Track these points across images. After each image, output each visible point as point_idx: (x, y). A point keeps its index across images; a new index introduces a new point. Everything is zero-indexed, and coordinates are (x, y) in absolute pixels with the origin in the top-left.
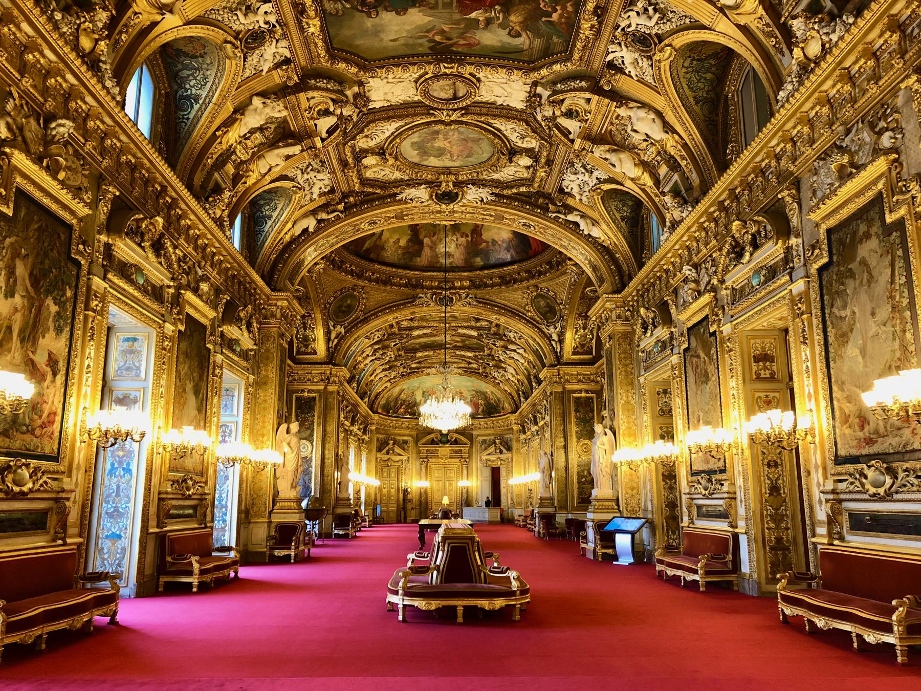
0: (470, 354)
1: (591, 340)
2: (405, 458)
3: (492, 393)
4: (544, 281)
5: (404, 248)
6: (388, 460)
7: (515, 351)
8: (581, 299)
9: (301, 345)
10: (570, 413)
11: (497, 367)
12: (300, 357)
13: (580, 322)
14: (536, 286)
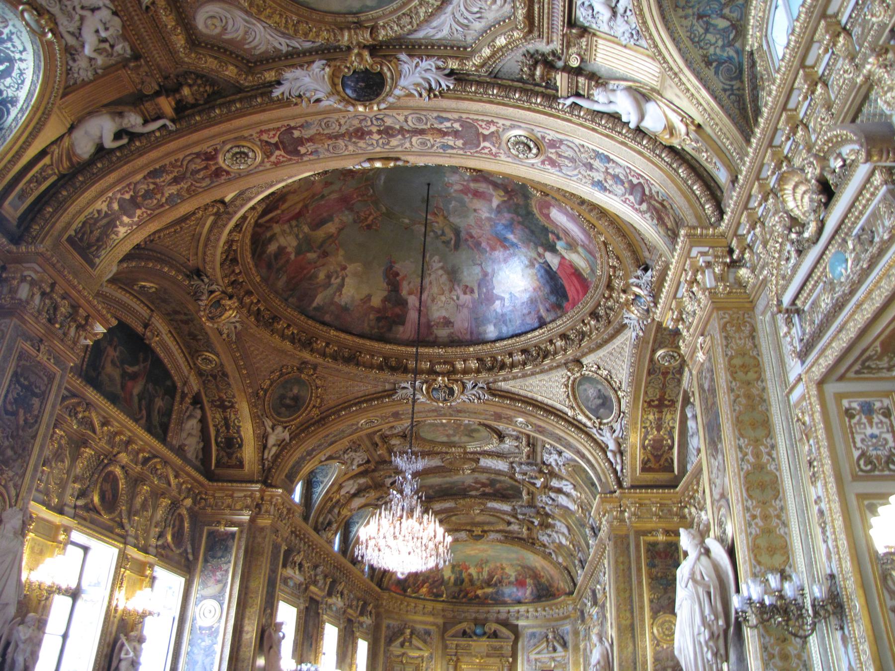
0: (506, 507)
1: (671, 447)
2: (426, 654)
3: (543, 568)
4: (591, 351)
5: (378, 311)
6: (404, 654)
7: (559, 491)
8: (649, 373)
9: (222, 453)
10: (639, 570)
11: (545, 526)
12: (219, 471)
13: (651, 417)
14: (578, 362)
